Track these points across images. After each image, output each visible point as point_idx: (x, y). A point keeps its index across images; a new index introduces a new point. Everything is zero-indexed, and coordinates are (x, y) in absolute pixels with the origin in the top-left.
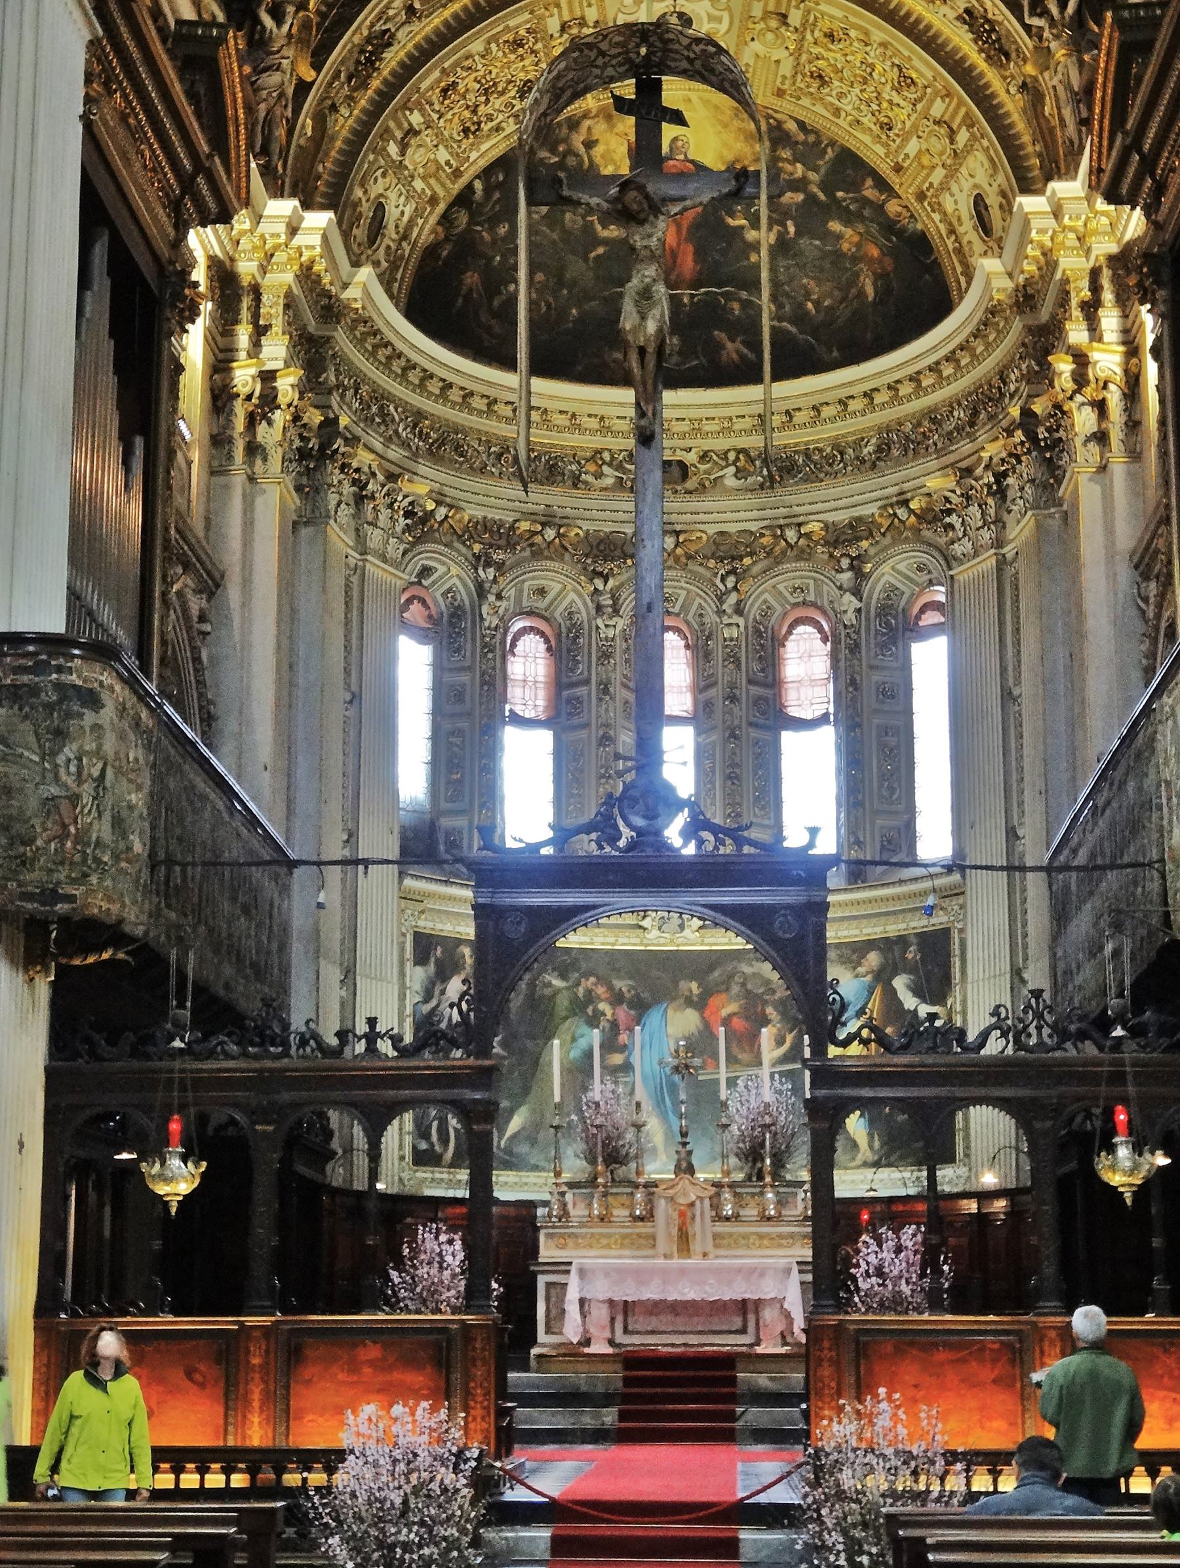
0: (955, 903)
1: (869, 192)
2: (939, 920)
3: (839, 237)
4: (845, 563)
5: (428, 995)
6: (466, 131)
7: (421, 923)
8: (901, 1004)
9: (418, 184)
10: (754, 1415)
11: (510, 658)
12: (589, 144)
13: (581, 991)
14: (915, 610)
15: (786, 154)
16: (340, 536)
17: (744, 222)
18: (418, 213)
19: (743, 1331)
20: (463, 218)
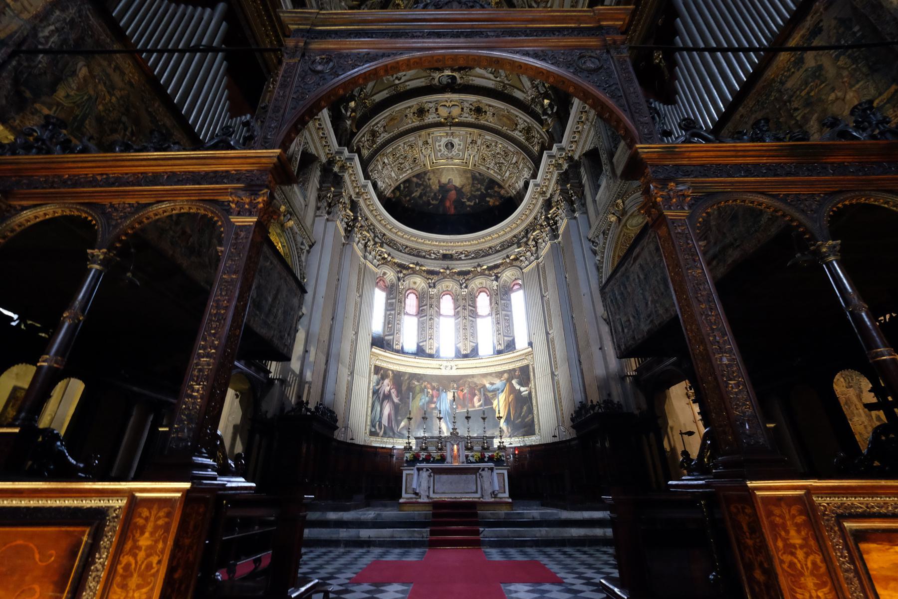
0: (530, 357)
1: (496, 189)
2: (525, 362)
3: (489, 201)
4: (493, 274)
5: (378, 384)
6: (399, 169)
7: (377, 363)
8: (515, 388)
9: (387, 181)
10: (487, 533)
11: (407, 299)
12: (429, 179)
13: (423, 386)
14: (512, 286)
15: (476, 182)
16: (358, 249)
17: (466, 200)
18: (386, 188)
19: (476, 492)
20: (398, 194)
